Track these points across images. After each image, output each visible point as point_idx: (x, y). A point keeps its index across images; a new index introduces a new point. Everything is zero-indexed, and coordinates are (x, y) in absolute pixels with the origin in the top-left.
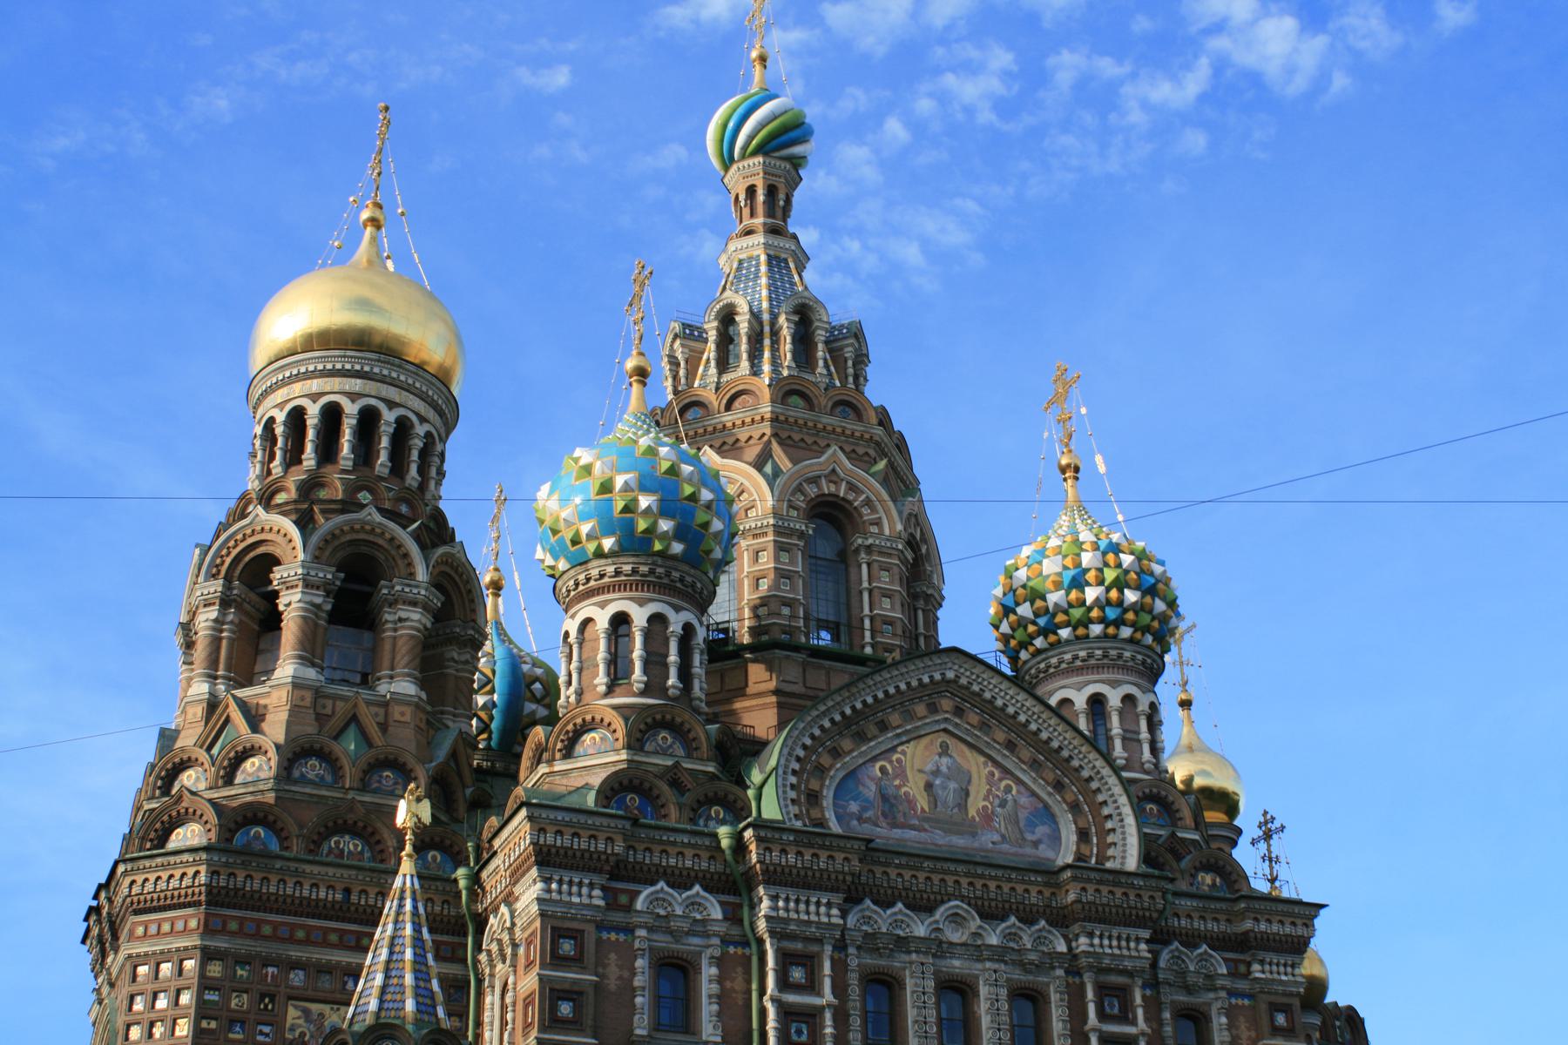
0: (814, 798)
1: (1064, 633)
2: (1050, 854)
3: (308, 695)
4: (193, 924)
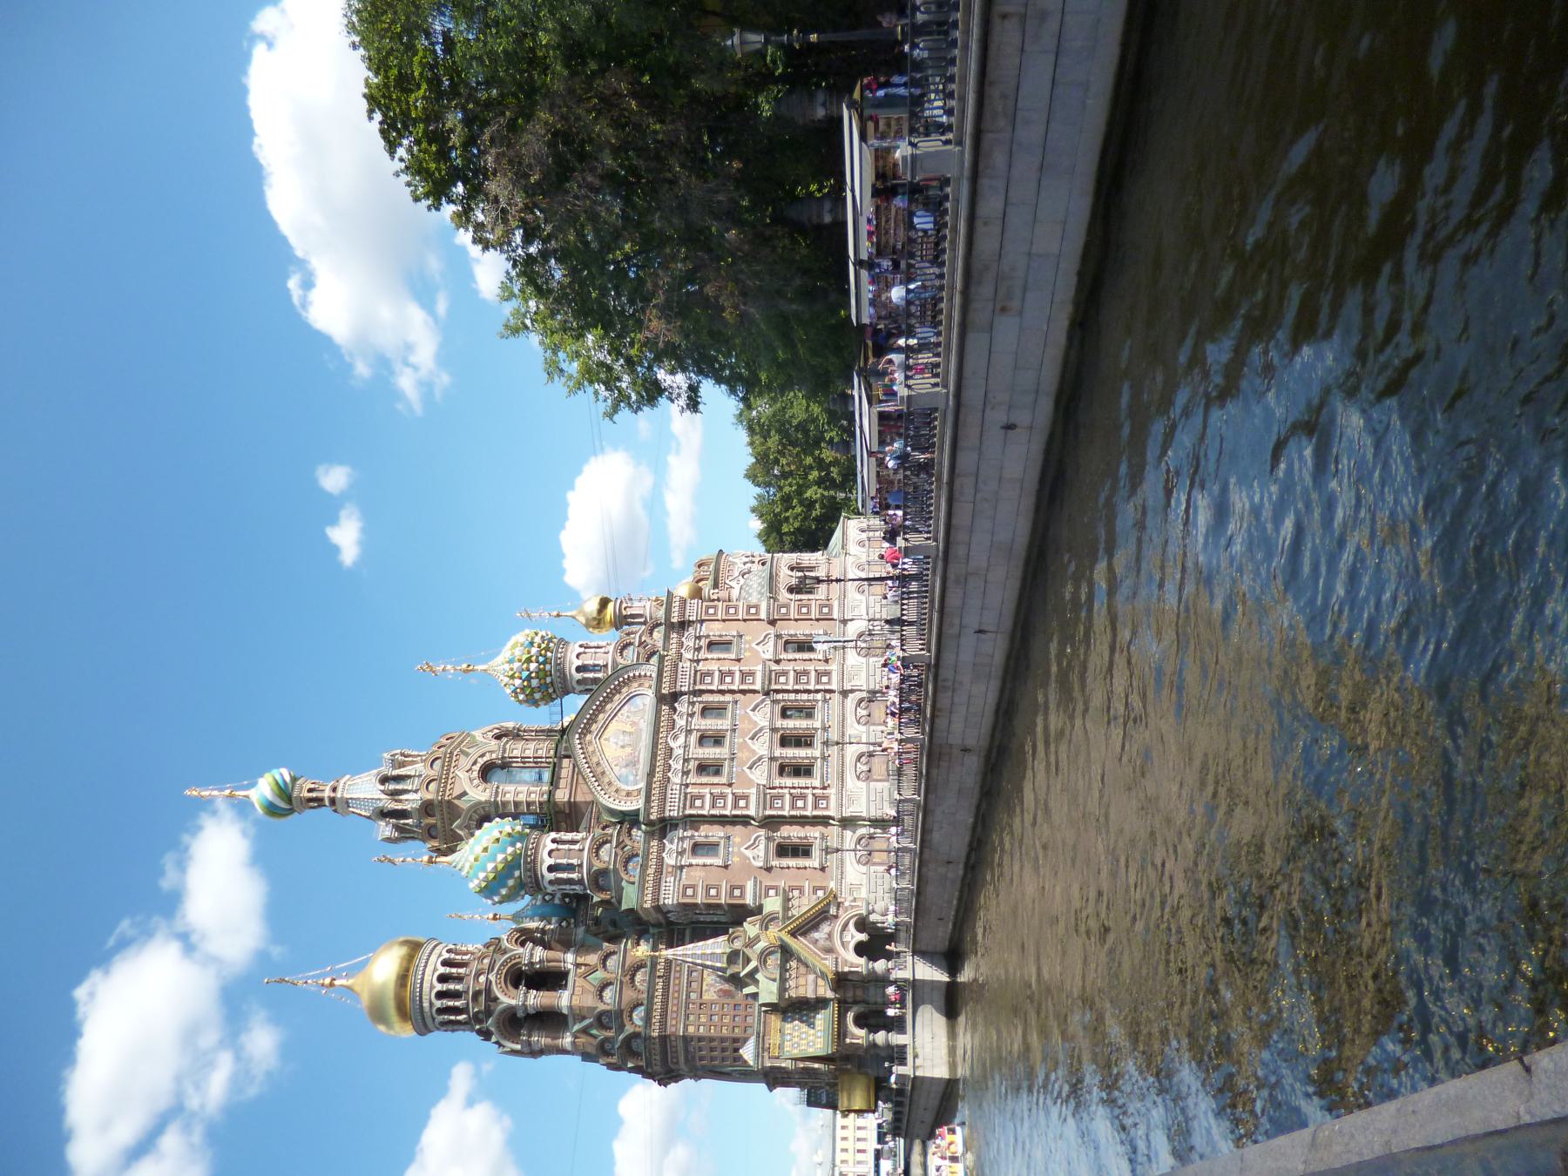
0: (628, 794)
1: (548, 680)
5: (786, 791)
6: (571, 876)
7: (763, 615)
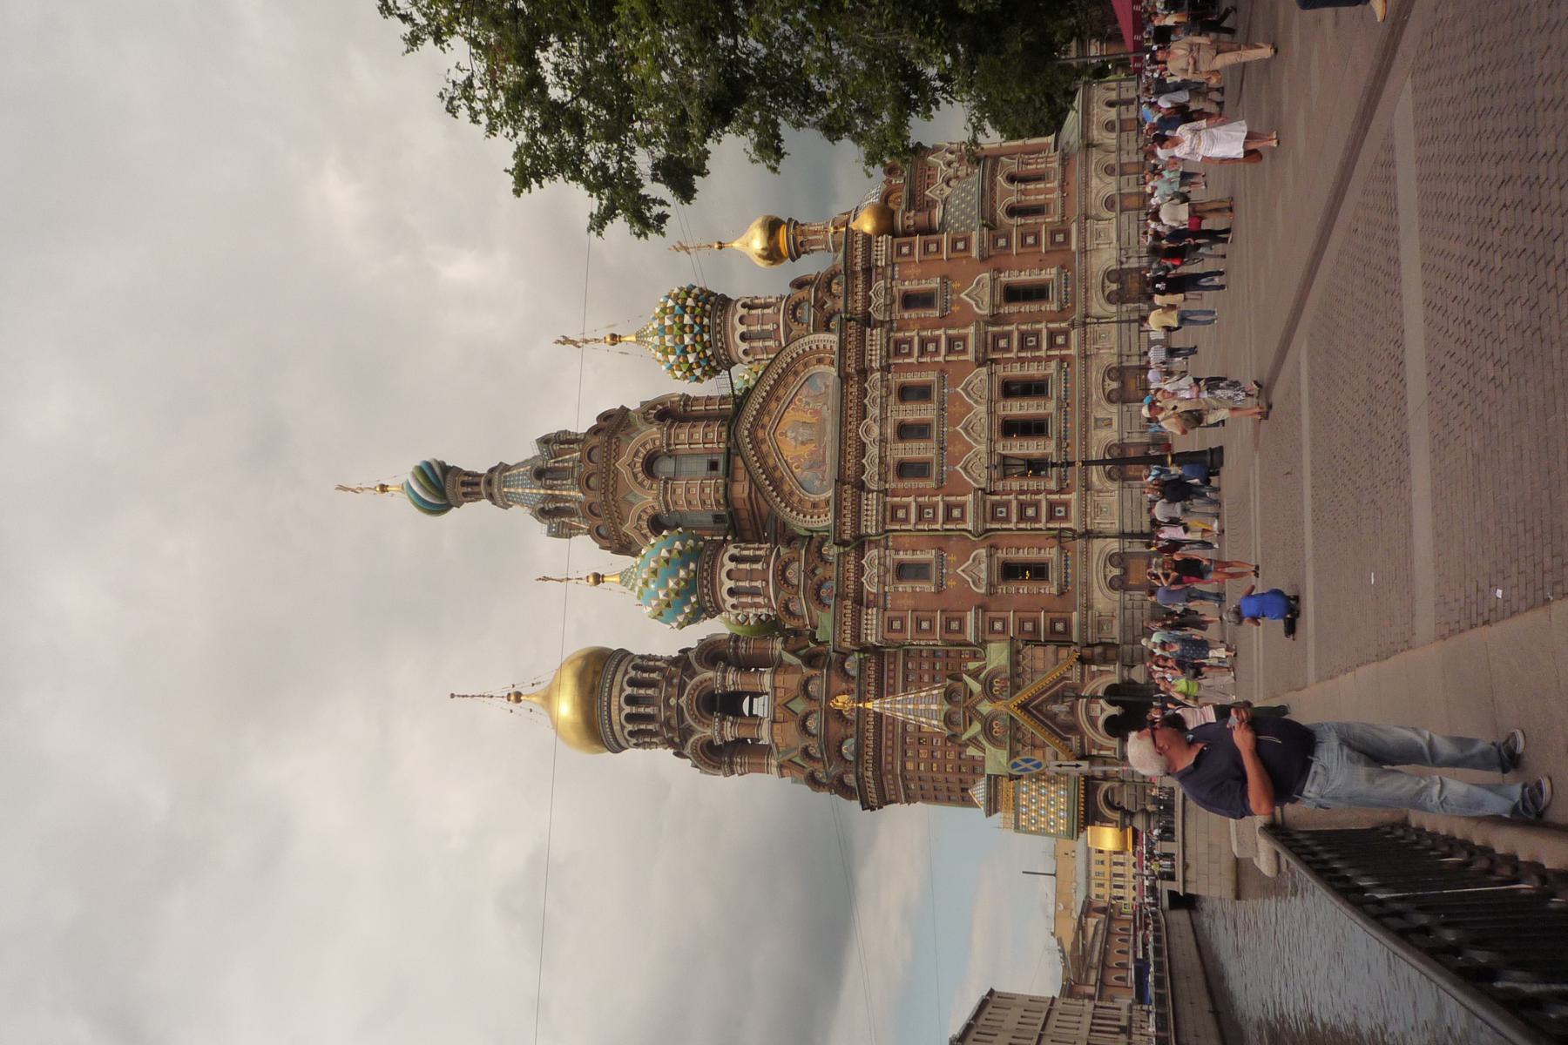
0: (815, 505)
1: (709, 352)
2: (831, 379)
3: (776, 726)
4: (890, 777)
5: (1012, 497)
6: (756, 600)
7: (975, 253)
